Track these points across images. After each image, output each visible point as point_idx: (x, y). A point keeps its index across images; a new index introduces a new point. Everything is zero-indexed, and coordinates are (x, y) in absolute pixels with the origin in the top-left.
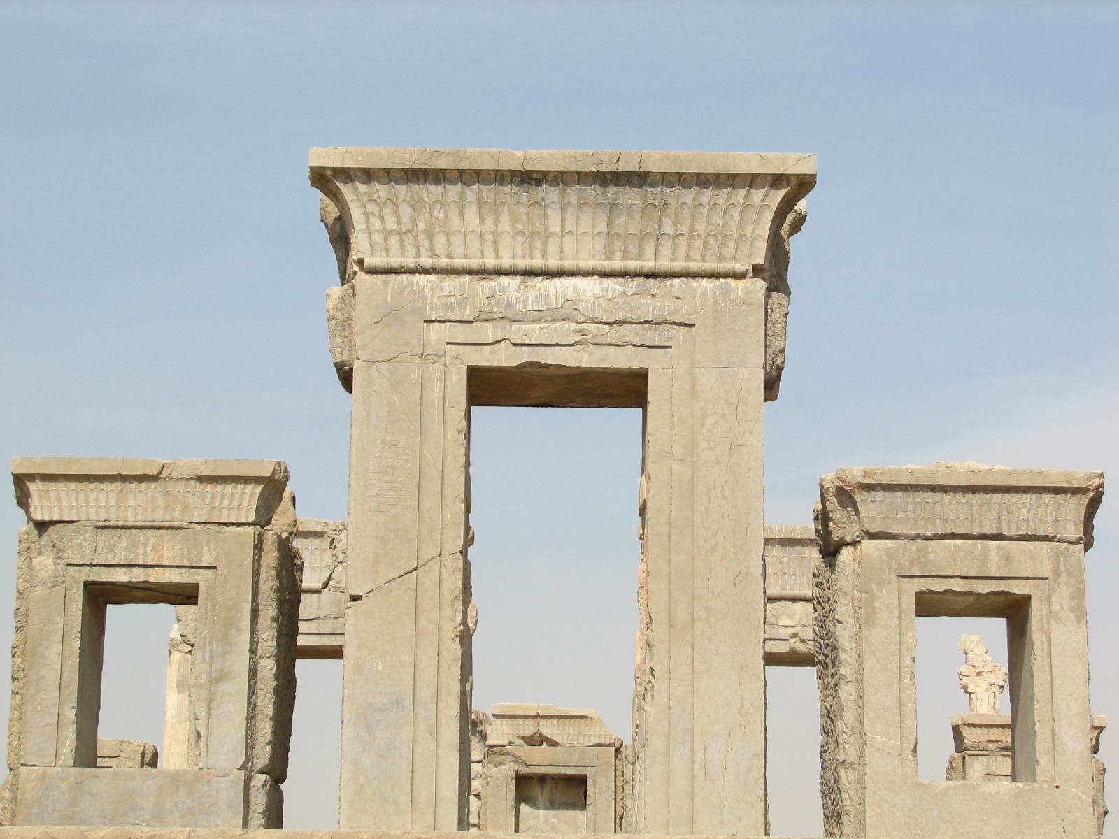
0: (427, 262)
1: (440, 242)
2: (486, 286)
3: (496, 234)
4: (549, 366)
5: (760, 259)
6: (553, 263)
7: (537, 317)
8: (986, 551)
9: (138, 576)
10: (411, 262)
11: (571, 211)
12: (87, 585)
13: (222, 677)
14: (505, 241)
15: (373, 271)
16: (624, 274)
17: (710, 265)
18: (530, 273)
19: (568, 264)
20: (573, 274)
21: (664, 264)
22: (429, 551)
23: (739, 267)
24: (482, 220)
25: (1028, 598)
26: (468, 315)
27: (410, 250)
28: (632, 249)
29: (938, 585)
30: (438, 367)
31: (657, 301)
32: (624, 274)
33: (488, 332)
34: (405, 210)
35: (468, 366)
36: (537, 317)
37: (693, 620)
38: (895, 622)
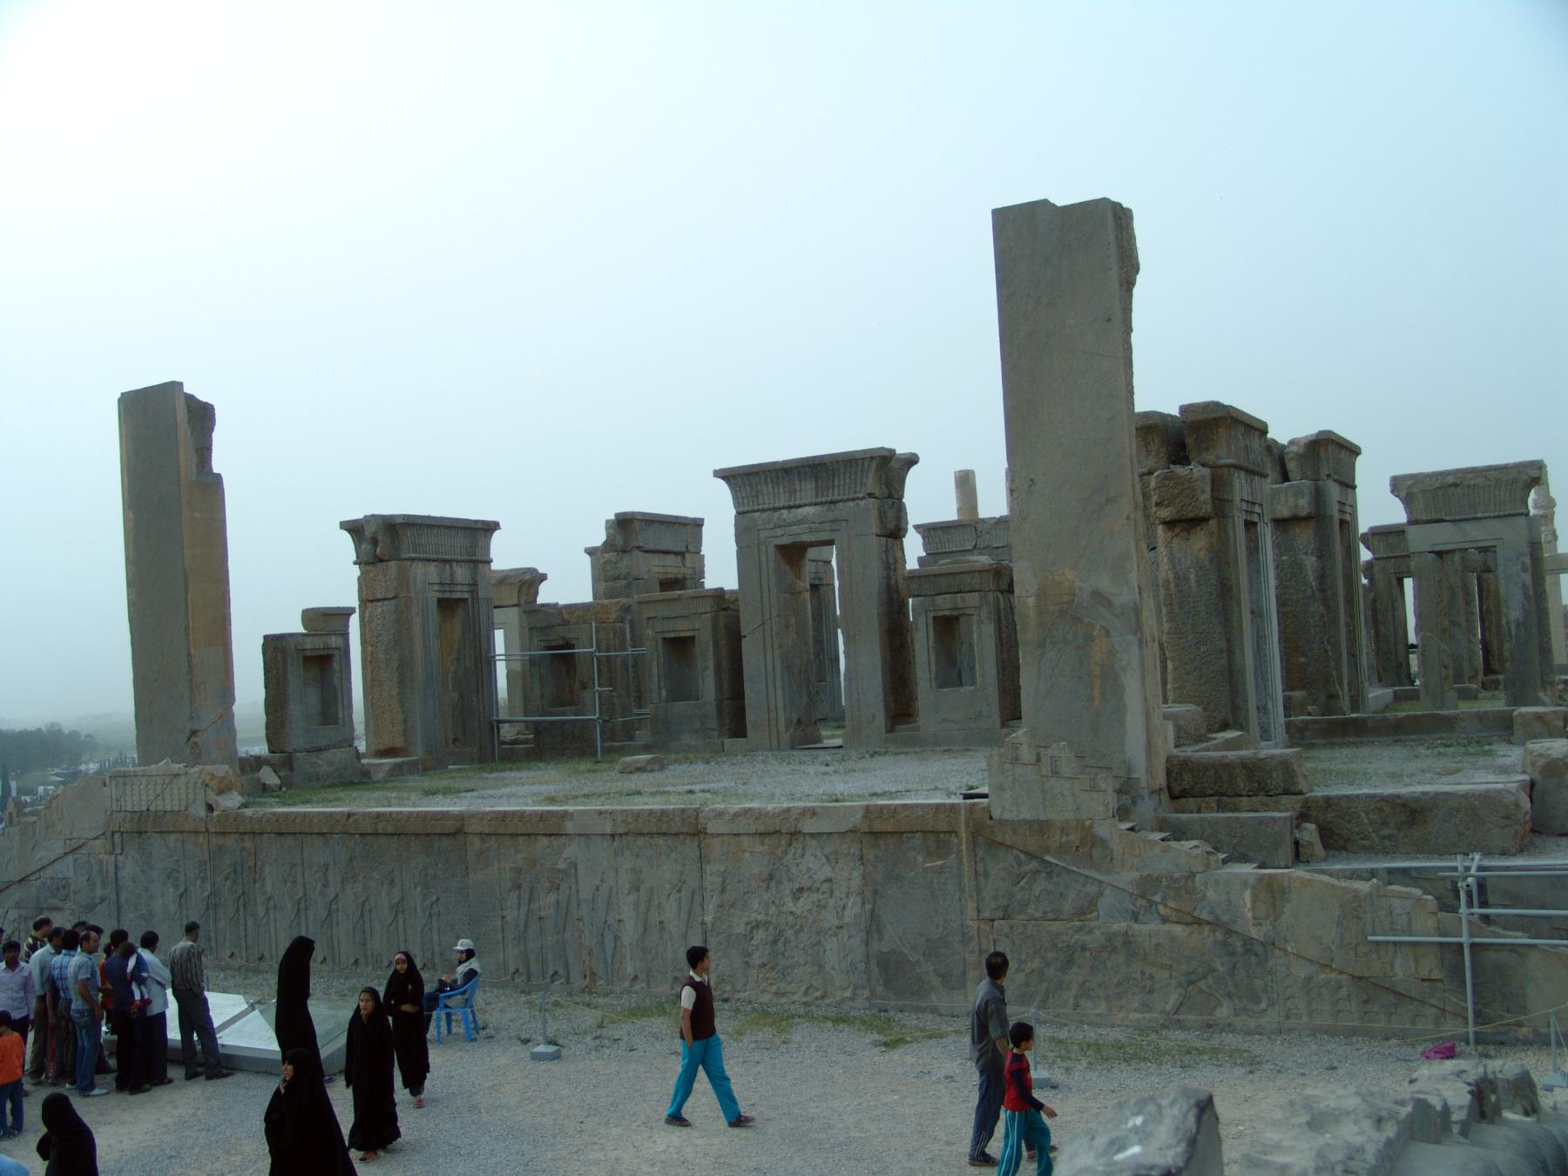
0: (756, 508)
1: (761, 498)
2: (776, 514)
3: (779, 493)
6: (797, 503)
10: (750, 509)
11: (803, 483)
13: (706, 668)
14: (782, 495)
18: (790, 507)
19: (802, 502)
20: (805, 505)
22: (767, 617)
23: (861, 495)
24: (773, 488)
26: (771, 526)
29: (940, 614)
30: (763, 548)
33: (779, 532)
34: (748, 488)
37: (855, 635)
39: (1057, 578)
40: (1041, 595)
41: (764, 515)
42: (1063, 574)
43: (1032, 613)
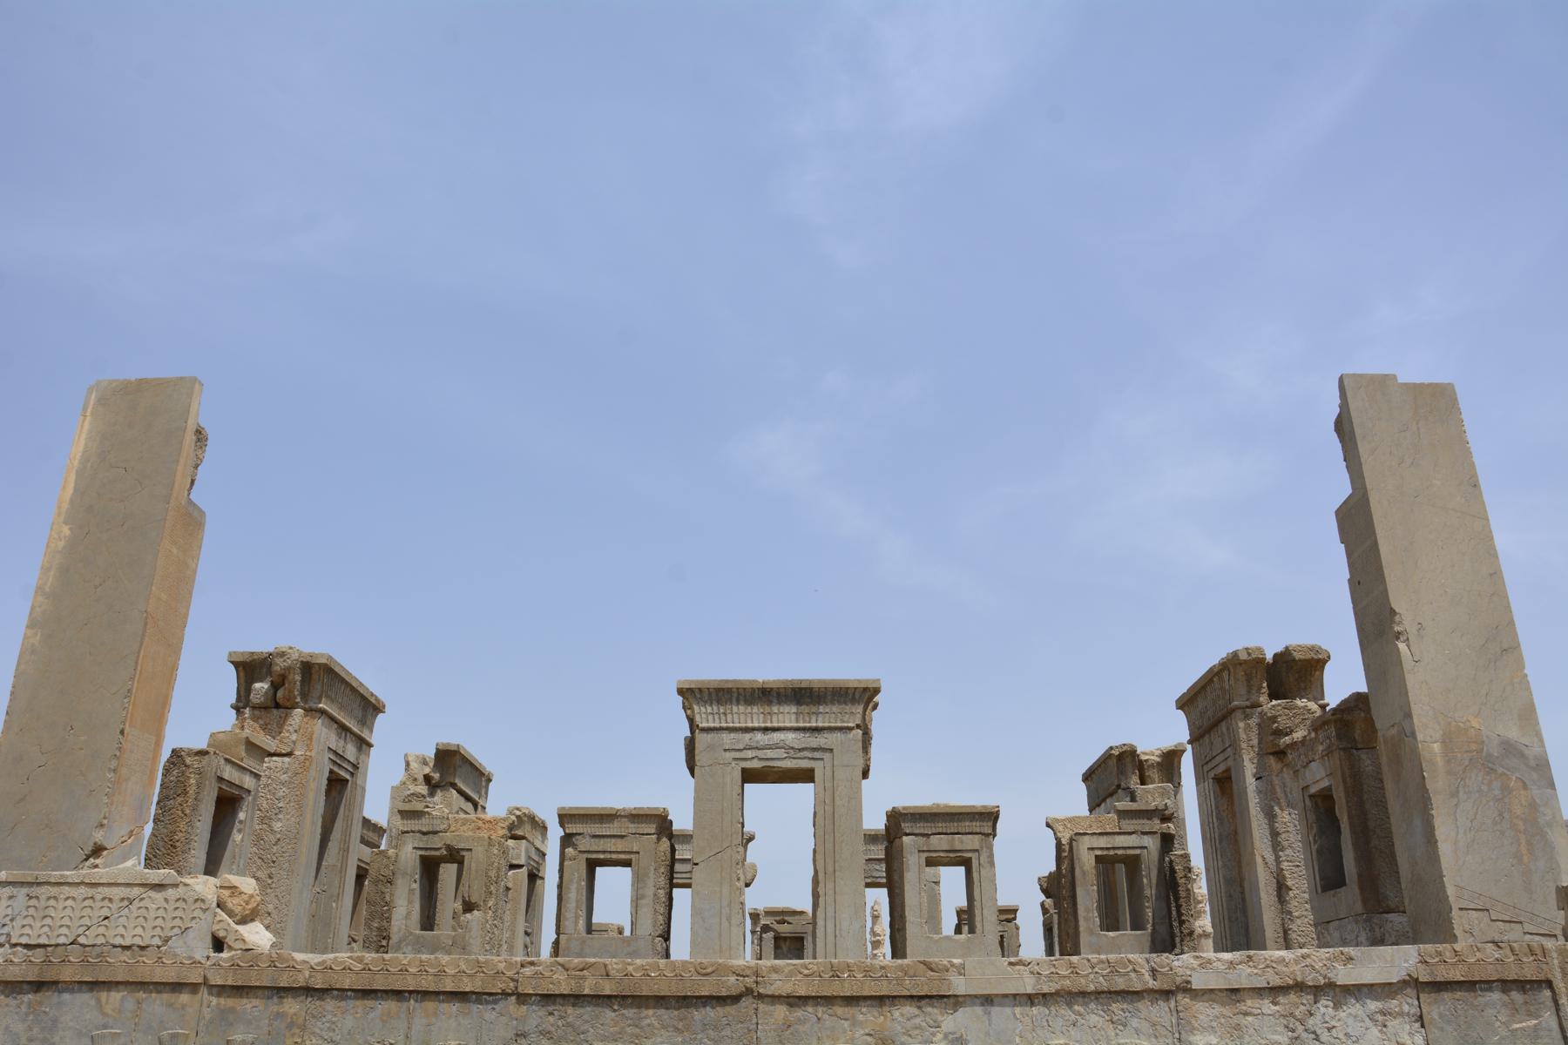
0: (724, 725)
1: (729, 717)
2: (748, 736)
4: (774, 767)
5: (858, 722)
6: (775, 725)
7: (769, 747)
8: (953, 839)
9: (608, 856)
10: (717, 725)
12: (587, 859)
13: (643, 897)
14: (755, 716)
15: (704, 730)
16: (804, 729)
17: (839, 725)
18: (766, 730)
19: (781, 725)
21: (820, 724)
25: (971, 858)
27: (717, 720)
28: (808, 719)
31: (818, 739)
32: (804, 729)
33: (750, 754)
34: (715, 708)
35: (742, 769)
36: (769, 747)
38: (917, 870)
39: (1462, 725)
40: (1446, 741)
41: (732, 735)
42: (1469, 721)
43: (1440, 761)
